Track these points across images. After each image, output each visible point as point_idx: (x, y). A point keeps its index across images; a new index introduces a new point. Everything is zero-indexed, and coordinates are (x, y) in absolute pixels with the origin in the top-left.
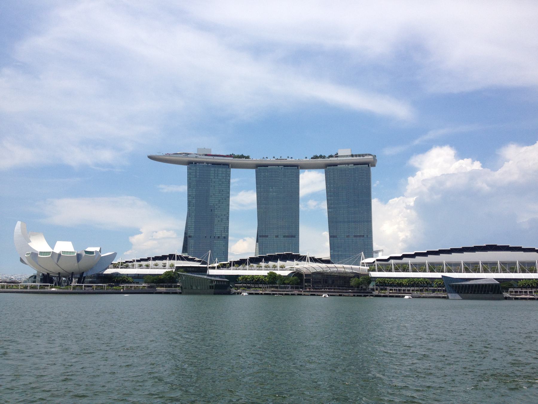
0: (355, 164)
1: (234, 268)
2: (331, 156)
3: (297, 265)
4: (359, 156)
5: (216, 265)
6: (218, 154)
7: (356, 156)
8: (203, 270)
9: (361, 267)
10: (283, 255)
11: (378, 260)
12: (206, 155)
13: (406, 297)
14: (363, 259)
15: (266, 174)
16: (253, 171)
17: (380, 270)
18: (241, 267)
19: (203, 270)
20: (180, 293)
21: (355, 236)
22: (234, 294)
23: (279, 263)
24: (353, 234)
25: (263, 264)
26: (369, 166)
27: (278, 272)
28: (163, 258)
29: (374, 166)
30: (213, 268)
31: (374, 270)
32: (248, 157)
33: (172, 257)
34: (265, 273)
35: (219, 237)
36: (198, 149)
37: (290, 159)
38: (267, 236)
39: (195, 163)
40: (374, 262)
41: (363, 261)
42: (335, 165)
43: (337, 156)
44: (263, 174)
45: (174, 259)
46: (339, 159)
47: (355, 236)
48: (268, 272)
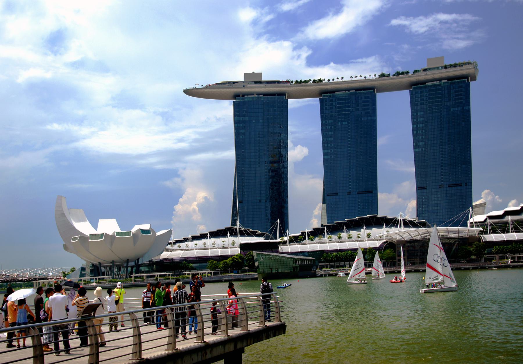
0: (450, 79)
1: (310, 241)
3: (388, 232)
8: (274, 247)
9: (469, 228)
11: (491, 217)
17: (494, 232)
18: (317, 239)
19: (274, 247)
22: (321, 276)
23: (364, 232)
30: (284, 243)
31: (486, 233)
40: (486, 220)
41: (471, 220)
45: (235, 235)
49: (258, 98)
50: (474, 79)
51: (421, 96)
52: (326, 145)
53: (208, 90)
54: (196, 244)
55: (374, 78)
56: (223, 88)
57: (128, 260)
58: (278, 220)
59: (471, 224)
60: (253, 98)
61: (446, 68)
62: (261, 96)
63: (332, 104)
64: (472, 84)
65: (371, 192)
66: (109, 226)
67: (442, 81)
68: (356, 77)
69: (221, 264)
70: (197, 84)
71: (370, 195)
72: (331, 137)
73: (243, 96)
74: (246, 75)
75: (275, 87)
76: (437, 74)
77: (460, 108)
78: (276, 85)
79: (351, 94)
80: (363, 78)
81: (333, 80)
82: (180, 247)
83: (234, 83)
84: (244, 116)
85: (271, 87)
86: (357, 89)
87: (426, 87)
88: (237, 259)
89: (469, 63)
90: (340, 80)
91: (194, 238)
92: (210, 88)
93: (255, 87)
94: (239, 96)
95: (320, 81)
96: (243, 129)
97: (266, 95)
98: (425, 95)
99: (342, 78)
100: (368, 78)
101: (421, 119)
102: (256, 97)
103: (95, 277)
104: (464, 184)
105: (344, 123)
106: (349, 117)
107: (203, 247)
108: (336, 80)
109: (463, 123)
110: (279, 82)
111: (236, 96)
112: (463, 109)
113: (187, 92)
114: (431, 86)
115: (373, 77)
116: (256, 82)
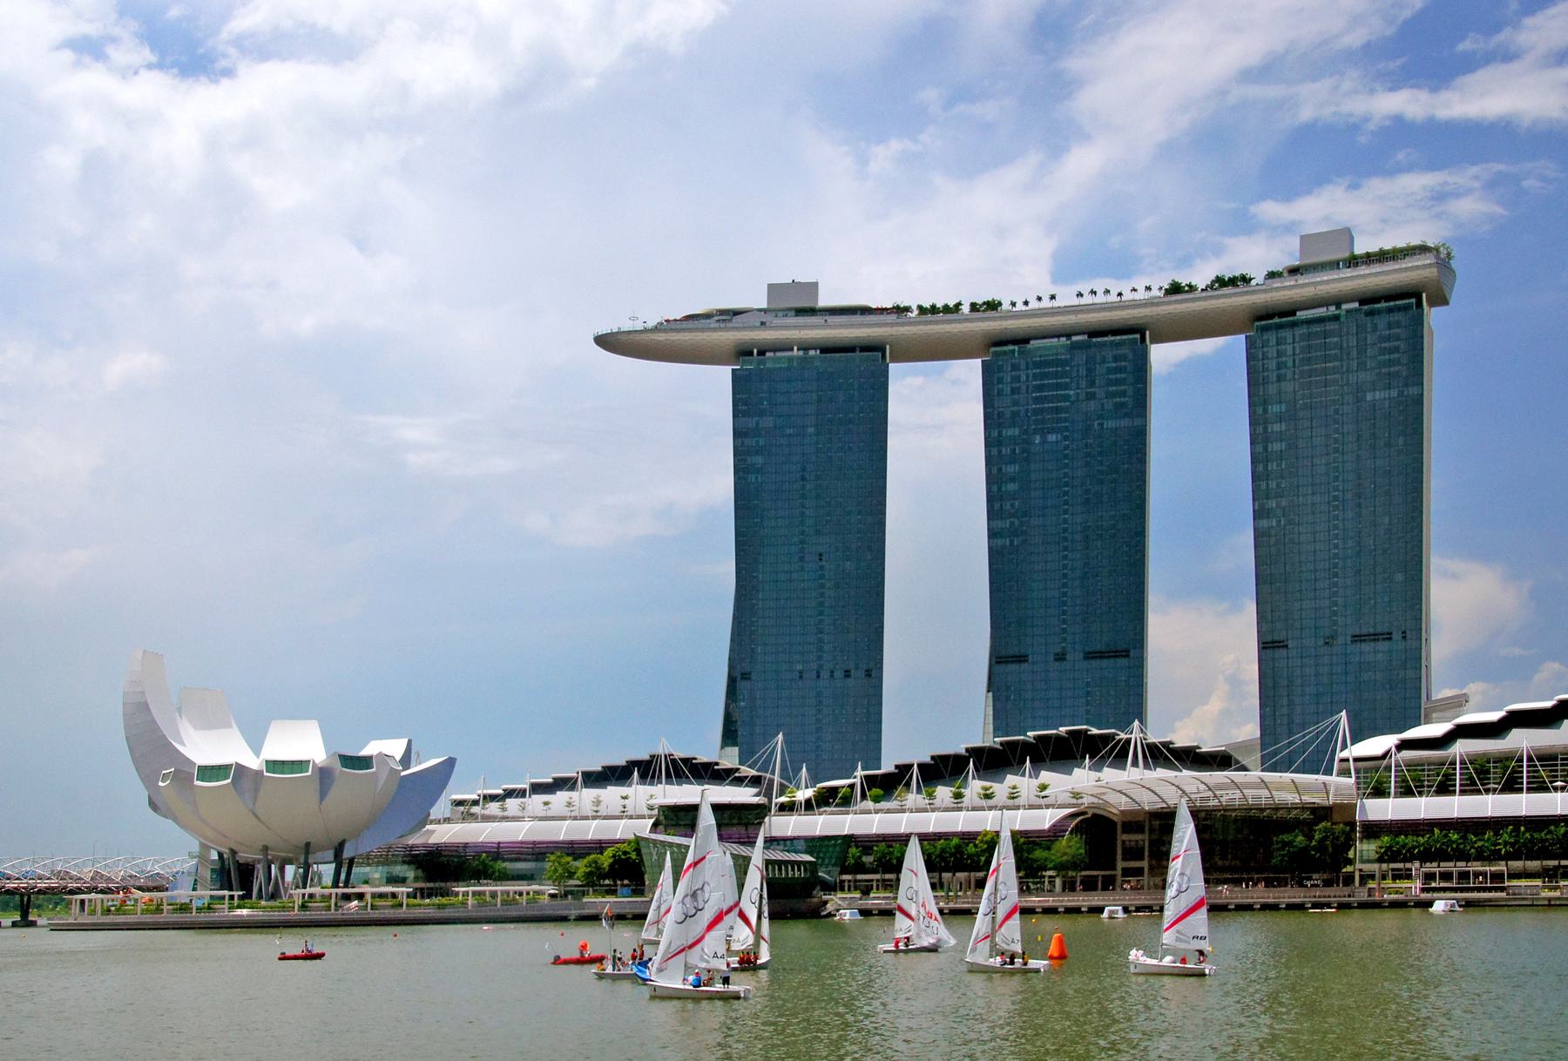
10: (1058, 738)
14: (1344, 747)
31: (1379, 792)
49: (804, 360)
50: (1440, 300)
51: (1279, 354)
52: (997, 506)
53: (661, 337)
54: (546, 804)
55: (1147, 295)
56: (702, 330)
57: (308, 845)
58: (780, 736)
59: (1344, 764)
60: (790, 359)
61: (1356, 265)
62: (812, 353)
63: (1017, 379)
64: (1434, 316)
65: (1125, 654)
66: (304, 743)
67: (1344, 307)
68: (1093, 292)
69: (581, 866)
70: (633, 319)
71: (1122, 662)
72: (1013, 480)
73: (762, 353)
74: (773, 289)
75: (852, 326)
76: (1327, 282)
77: (1394, 393)
78: (858, 318)
79: (1075, 347)
80: (1113, 298)
81: (1026, 303)
82: (504, 809)
83: (736, 313)
84: (762, 414)
85: (841, 326)
86: (1094, 333)
87: (1294, 324)
88: (625, 853)
89: (1423, 249)
90: (1046, 303)
91: (538, 788)
92: (665, 331)
93: (796, 327)
94: (751, 354)
95: (993, 306)
96: (757, 453)
97: (828, 349)
98: (1289, 349)
99: (1053, 297)
100: (1128, 296)
101: (1276, 427)
102: (798, 358)
103: (226, 893)
104: (1396, 636)
105: (1052, 438)
106: (1066, 420)
107: (566, 812)
108: (1034, 304)
109: (1401, 440)
110: (865, 311)
111: (743, 352)
112: (1401, 394)
113: (607, 342)
114: (1309, 322)
115: (1141, 295)
116: (801, 312)
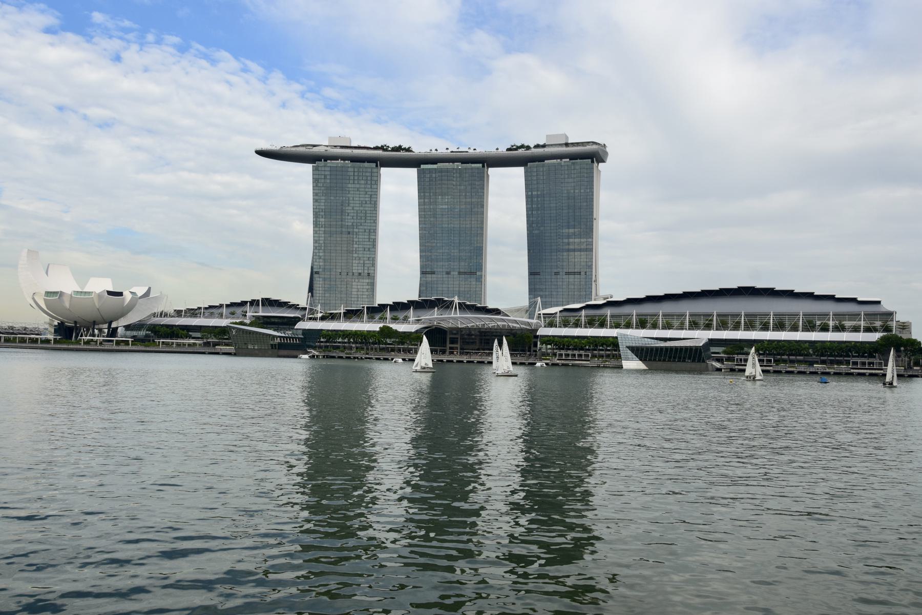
2: (537, 146)
4: (578, 144)
5: (320, 315)
6: (362, 145)
7: (573, 144)
12: (342, 147)
13: (538, 364)
15: (434, 175)
16: (412, 173)
20: (235, 355)
21: (568, 273)
24: (565, 270)
25: (388, 314)
26: (593, 162)
27: (395, 326)
28: (243, 304)
29: (603, 161)
32: (408, 150)
33: (254, 303)
34: (375, 327)
35: (360, 274)
36: (330, 138)
37: (471, 151)
38: (433, 273)
39: (325, 160)
42: (541, 159)
43: (544, 146)
44: (428, 176)
46: (547, 150)
47: (568, 273)
48: (381, 325)
